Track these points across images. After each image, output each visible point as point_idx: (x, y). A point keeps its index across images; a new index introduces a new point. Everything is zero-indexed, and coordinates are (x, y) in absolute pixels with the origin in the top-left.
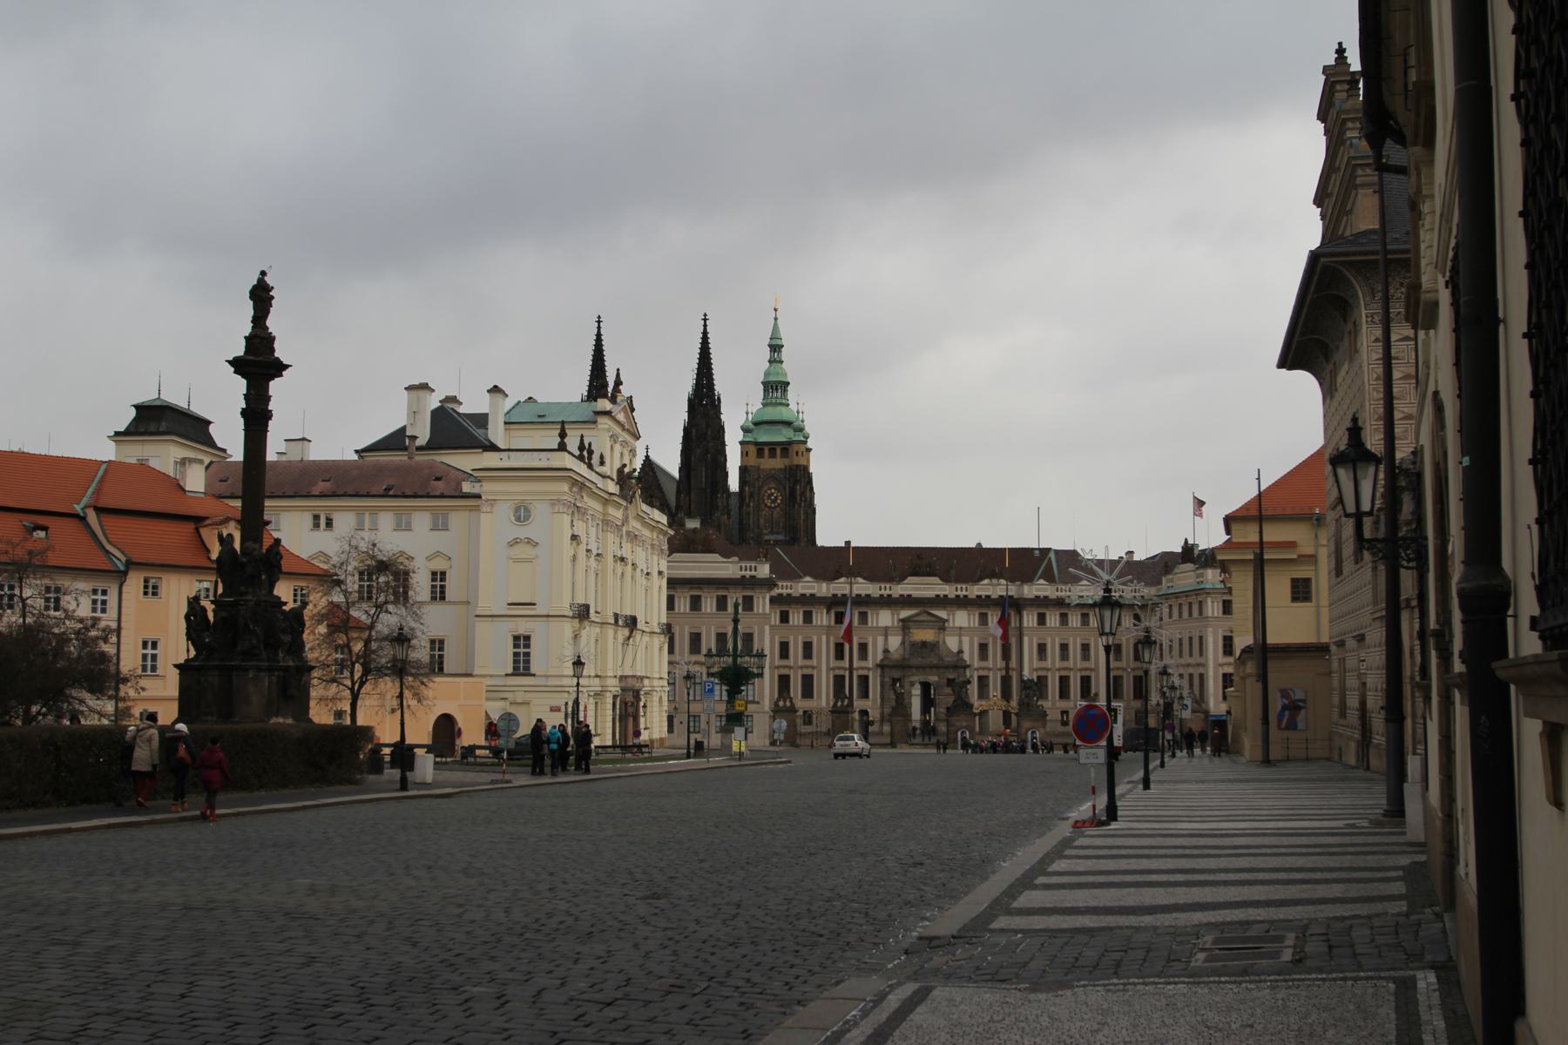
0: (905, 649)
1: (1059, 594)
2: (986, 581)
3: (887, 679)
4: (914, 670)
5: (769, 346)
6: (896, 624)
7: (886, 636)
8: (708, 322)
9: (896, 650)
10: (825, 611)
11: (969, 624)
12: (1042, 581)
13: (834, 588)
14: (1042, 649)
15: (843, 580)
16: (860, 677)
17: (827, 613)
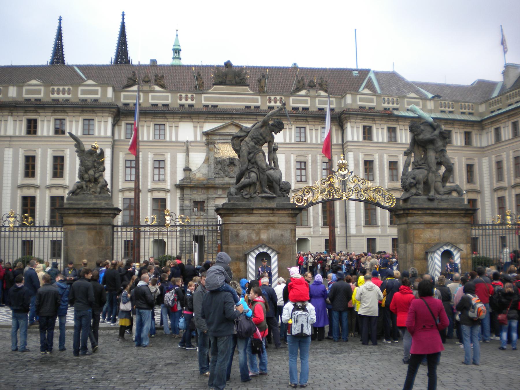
0: (209, 166)
1: (386, 105)
2: (303, 92)
3: (187, 203)
4: (220, 192)
5: (174, 50)
6: (199, 139)
7: (187, 151)
8: (125, 17)
9: (199, 169)
10: (110, 120)
11: (285, 139)
12: (366, 91)
13: (125, 97)
14: (369, 165)
15: (135, 88)
16: (155, 200)
17: (114, 126)
